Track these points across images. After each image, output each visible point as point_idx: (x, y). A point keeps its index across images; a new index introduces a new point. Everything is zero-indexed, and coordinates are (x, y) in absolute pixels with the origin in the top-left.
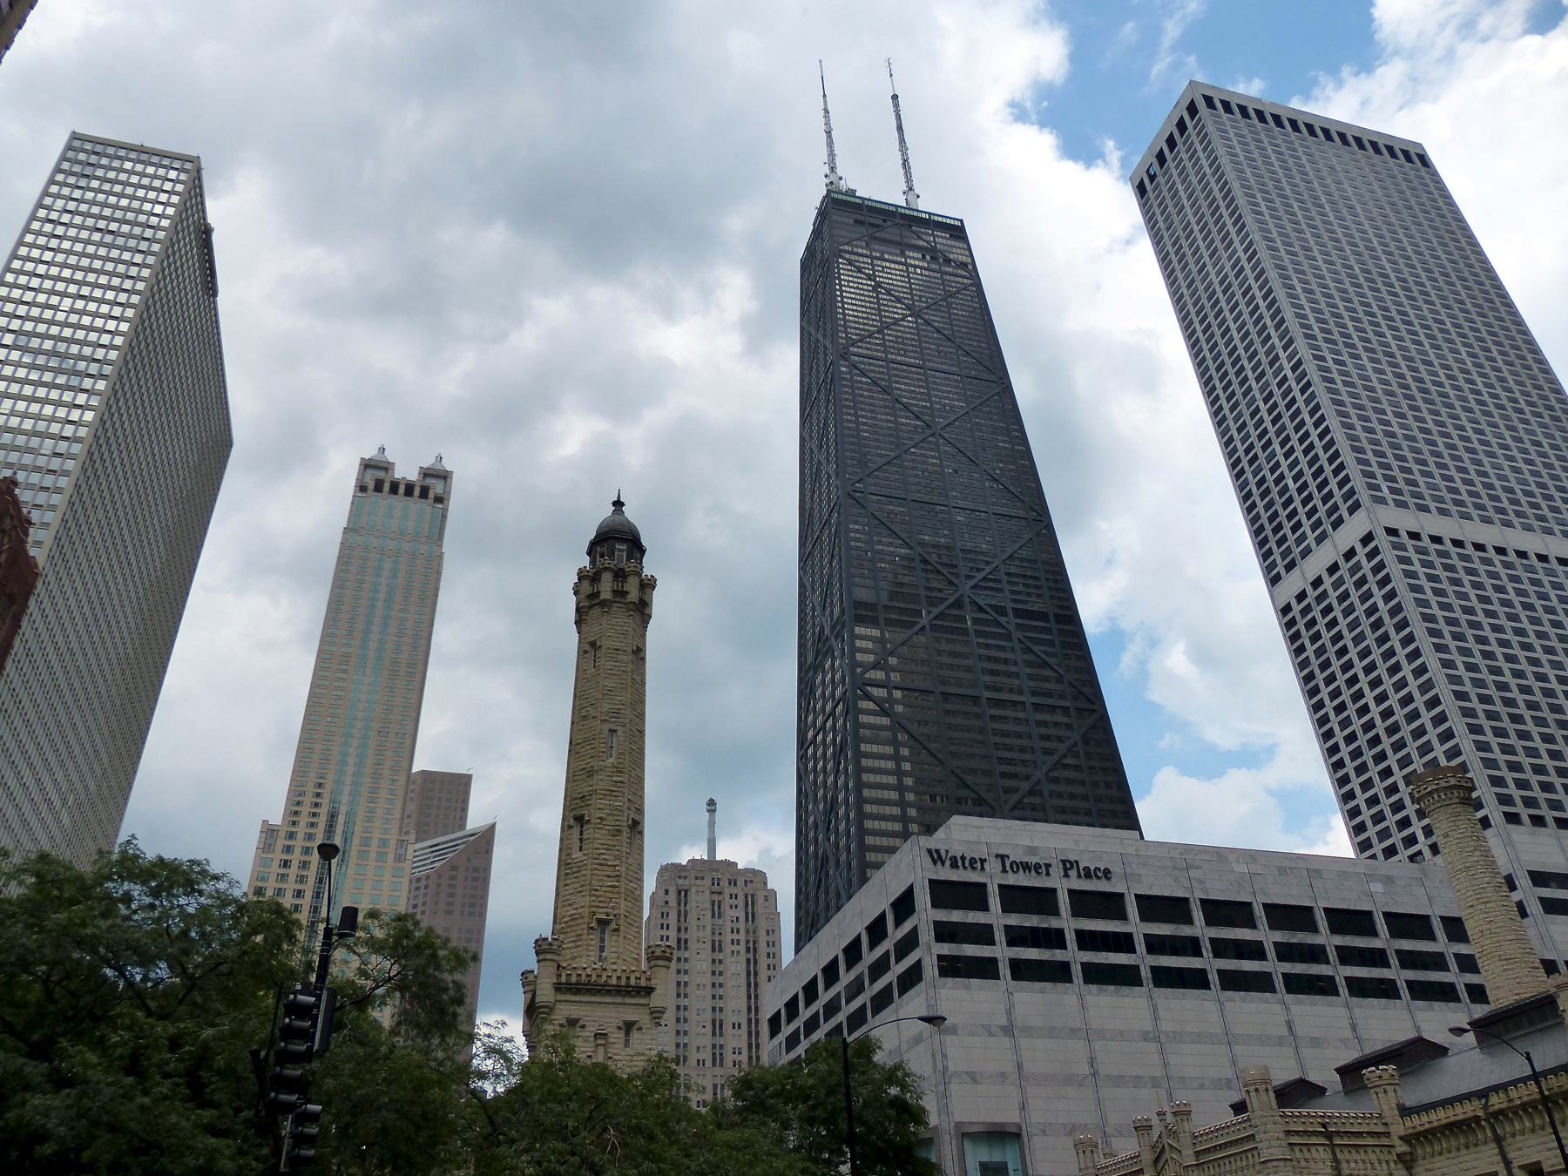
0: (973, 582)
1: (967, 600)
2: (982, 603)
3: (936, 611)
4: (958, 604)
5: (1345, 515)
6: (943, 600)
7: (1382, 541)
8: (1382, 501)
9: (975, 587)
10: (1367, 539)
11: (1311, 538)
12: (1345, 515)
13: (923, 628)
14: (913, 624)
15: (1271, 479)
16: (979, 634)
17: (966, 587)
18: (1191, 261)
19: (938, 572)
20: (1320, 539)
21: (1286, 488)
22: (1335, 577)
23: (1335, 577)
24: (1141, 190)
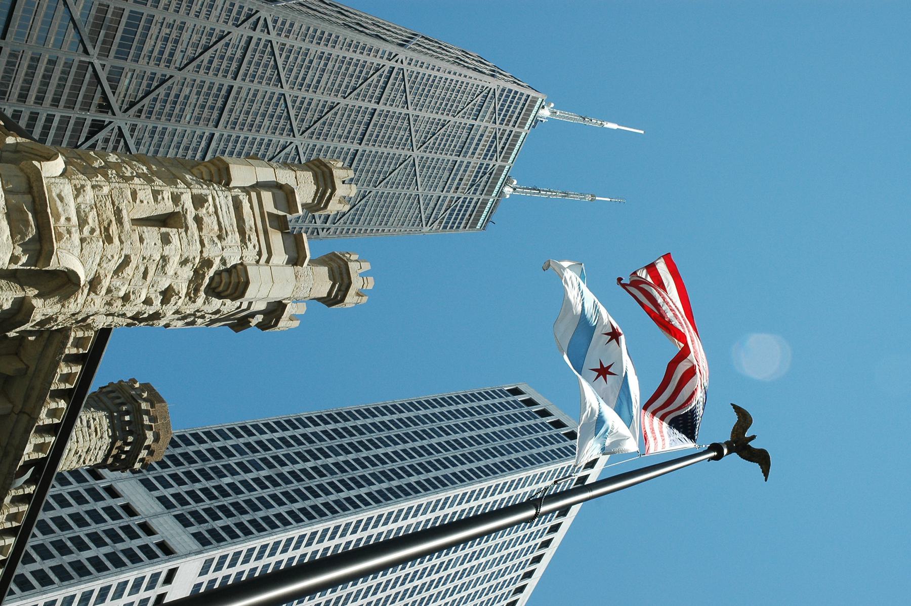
0: (127, 134)
1: (106, 118)
2: (101, 136)
3: (103, 76)
4: (106, 107)
5: (193, 529)
6: (114, 88)
7: (163, 568)
8: (204, 571)
9: (121, 134)
10: (166, 550)
11: (167, 493)
12: (193, 529)
13: (86, 52)
14: (94, 42)
15: (232, 461)
16: (65, 121)
17: (122, 121)
18: (452, 423)
19: (147, 94)
20: (163, 500)
21: (221, 475)
22: (120, 511)
23: (120, 511)
24: (516, 392)
